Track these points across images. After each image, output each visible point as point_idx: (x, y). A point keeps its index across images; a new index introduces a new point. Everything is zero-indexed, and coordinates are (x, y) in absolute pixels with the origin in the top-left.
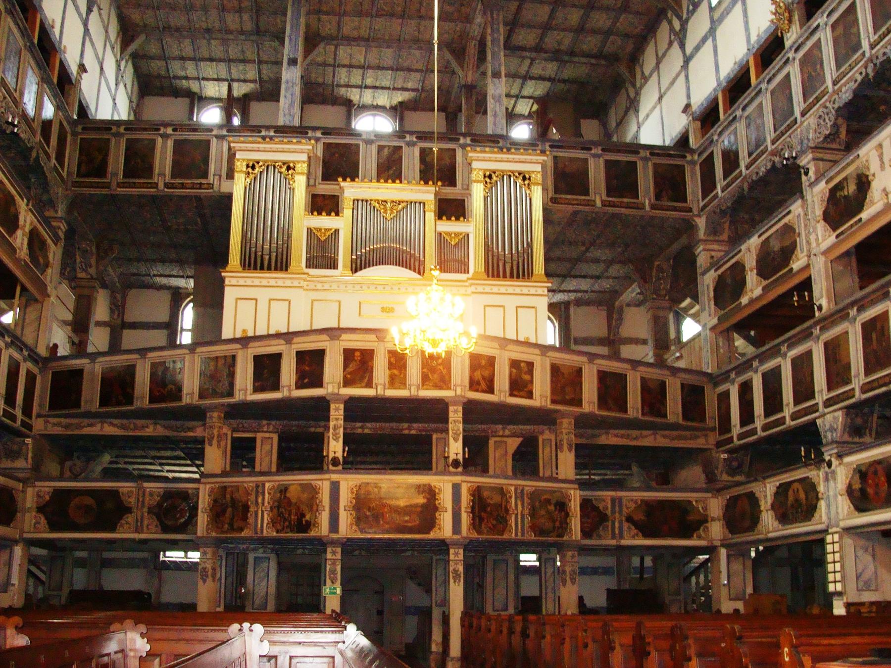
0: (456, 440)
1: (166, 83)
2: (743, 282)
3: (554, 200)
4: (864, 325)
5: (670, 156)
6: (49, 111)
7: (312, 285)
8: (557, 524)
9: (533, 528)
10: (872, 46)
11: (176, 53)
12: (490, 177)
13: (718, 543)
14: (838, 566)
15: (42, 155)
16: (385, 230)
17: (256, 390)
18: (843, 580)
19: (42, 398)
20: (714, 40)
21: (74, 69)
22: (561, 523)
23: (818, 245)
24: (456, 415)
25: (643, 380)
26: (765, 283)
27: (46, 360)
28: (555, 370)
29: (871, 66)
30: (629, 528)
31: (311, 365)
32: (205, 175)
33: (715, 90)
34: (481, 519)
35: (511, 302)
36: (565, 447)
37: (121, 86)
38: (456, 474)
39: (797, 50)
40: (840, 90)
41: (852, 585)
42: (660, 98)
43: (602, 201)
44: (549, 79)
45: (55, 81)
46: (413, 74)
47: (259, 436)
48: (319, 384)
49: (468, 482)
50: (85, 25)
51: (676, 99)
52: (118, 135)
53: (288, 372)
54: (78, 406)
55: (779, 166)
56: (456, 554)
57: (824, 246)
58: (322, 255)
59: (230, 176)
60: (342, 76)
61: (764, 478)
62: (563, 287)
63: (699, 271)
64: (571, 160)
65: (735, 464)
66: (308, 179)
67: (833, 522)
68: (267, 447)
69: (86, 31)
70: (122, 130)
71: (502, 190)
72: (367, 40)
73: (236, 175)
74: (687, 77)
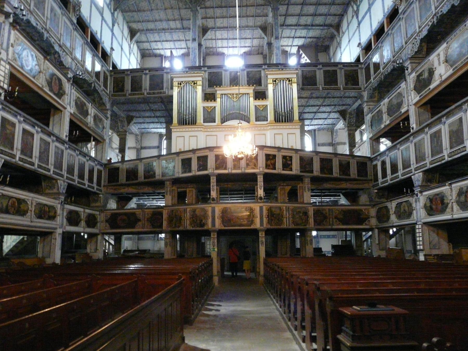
0: (261, 189)
2: (382, 118)
3: (302, 89)
4: (431, 136)
5: (352, 66)
6: (98, 68)
7: (206, 130)
8: (304, 221)
9: (293, 222)
10: (436, 8)
11: (153, 40)
12: (275, 81)
13: (374, 227)
14: (421, 239)
15: (96, 85)
16: (234, 106)
18: (423, 244)
20: (370, 13)
21: (108, 50)
22: (305, 221)
23: (412, 101)
24: (260, 179)
25: (340, 161)
26: (390, 118)
29: (435, 18)
30: (336, 221)
31: (203, 161)
32: (163, 89)
33: (370, 36)
34: (272, 220)
35: (285, 132)
36: (307, 190)
38: (260, 203)
39: (404, 14)
40: (422, 30)
41: (427, 247)
42: (349, 41)
43: (323, 88)
44: (304, 37)
45: (100, 56)
46: (248, 40)
47: (188, 190)
48: (206, 169)
49: (266, 206)
50: (112, 31)
51: (355, 41)
53: (194, 164)
55: (395, 67)
56: (262, 234)
57: (415, 101)
58: (209, 117)
59: (172, 88)
60: (219, 43)
61: (391, 201)
62: (312, 123)
63: (365, 114)
64: (309, 71)
65: (381, 194)
66: (203, 87)
67: (419, 220)
68: (191, 194)
69: (113, 34)
70: (129, 73)
71: (280, 86)
72: (227, 28)
73: (174, 88)
74: (359, 31)
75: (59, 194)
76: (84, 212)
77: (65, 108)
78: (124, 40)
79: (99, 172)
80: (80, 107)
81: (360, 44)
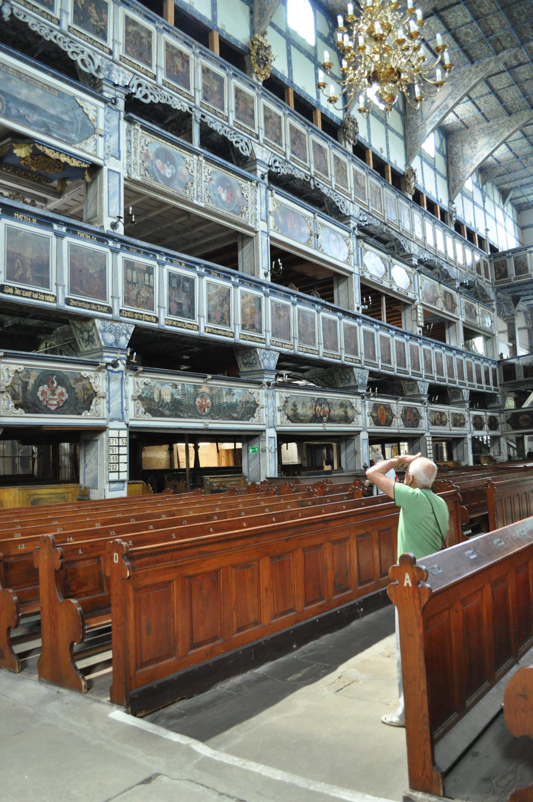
1: (529, 204)
19: (500, 374)
27: (499, 362)
37: (507, 218)
54: (515, 379)
75: (464, 402)
76: (486, 415)
77: (458, 319)
78: (496, 207)
79: (494, 371)
80: (470, 311)
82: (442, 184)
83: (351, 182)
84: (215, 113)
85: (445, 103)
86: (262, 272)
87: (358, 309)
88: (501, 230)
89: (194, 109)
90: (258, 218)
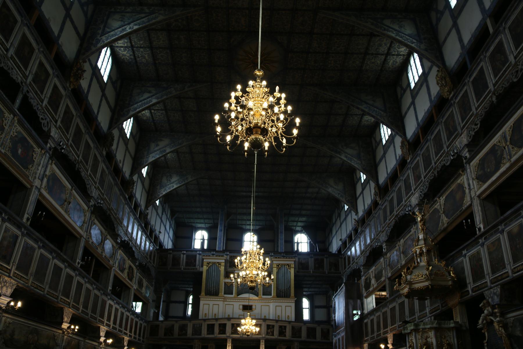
3: (298, 272)
17: (208, 334)
28: (293, 328)
32: (195, 266)
35: (284, 305)
42: (336, 233)
52: (170, 254)
53: (217, 329)
59: (202, 266)
73: (204, 267)
77: (133, 287)
79: (145, 327)
81: (341, 240)
82: (145, 195)
83: (99, 175)
84: (36, 93)
85: (164, 149)
86: (26, 216)
87: (79, 263)
88: (167, 235)
89: (24, 84)
90: (37, 176)
